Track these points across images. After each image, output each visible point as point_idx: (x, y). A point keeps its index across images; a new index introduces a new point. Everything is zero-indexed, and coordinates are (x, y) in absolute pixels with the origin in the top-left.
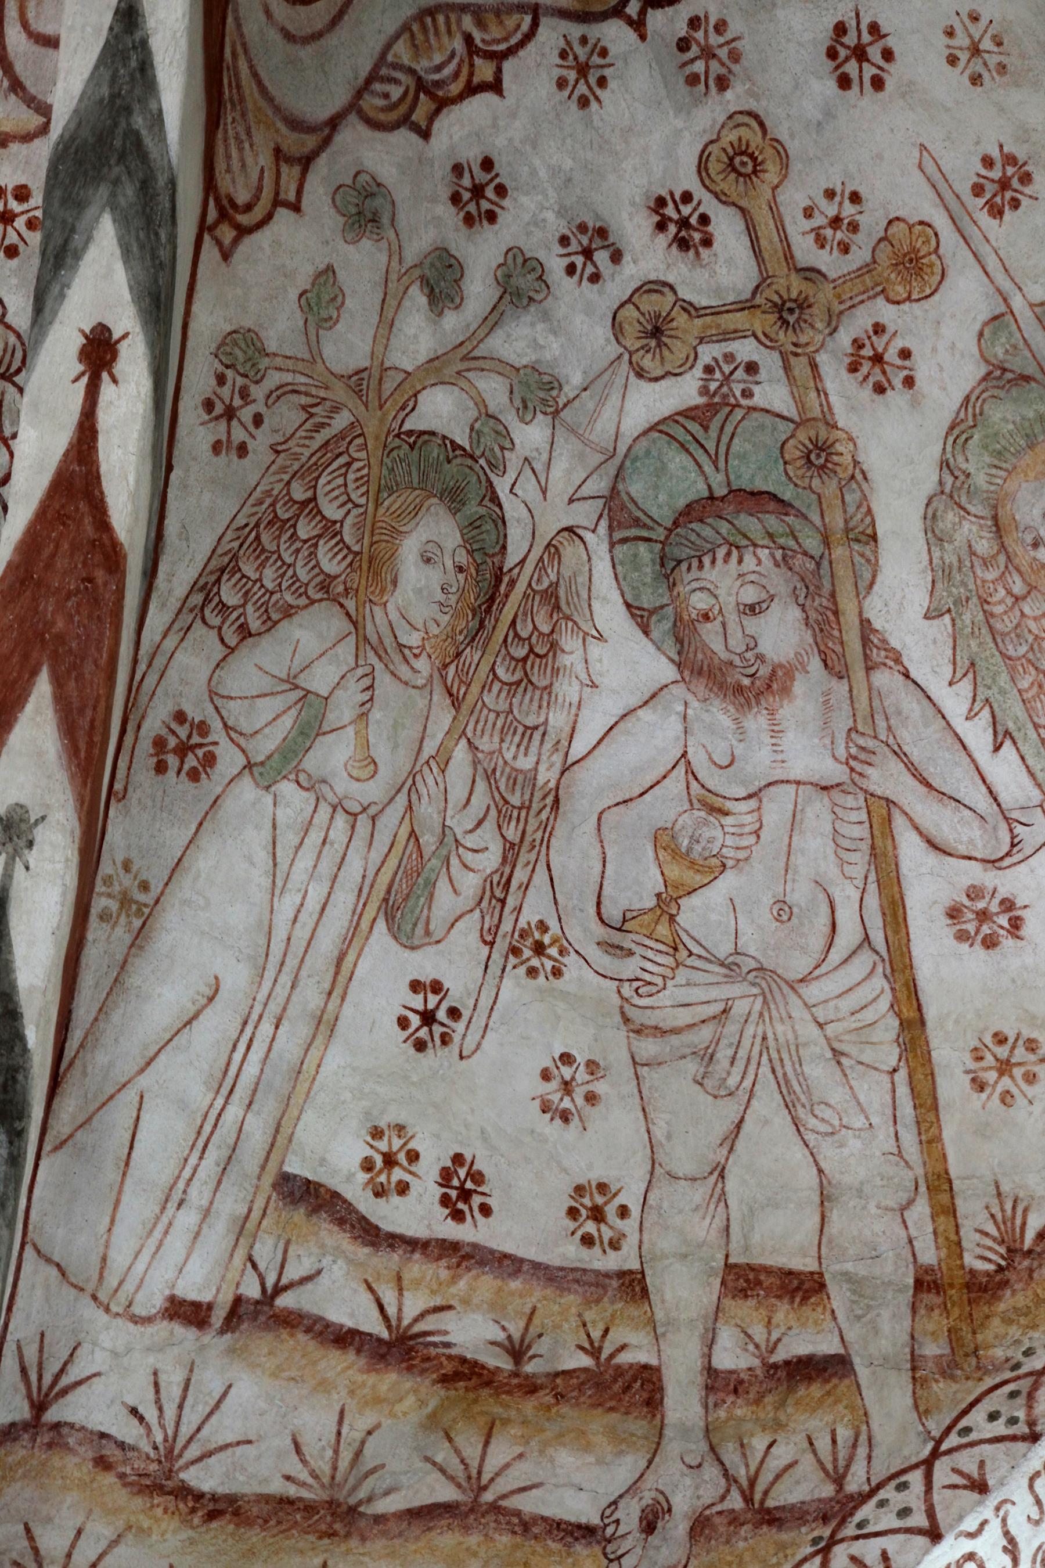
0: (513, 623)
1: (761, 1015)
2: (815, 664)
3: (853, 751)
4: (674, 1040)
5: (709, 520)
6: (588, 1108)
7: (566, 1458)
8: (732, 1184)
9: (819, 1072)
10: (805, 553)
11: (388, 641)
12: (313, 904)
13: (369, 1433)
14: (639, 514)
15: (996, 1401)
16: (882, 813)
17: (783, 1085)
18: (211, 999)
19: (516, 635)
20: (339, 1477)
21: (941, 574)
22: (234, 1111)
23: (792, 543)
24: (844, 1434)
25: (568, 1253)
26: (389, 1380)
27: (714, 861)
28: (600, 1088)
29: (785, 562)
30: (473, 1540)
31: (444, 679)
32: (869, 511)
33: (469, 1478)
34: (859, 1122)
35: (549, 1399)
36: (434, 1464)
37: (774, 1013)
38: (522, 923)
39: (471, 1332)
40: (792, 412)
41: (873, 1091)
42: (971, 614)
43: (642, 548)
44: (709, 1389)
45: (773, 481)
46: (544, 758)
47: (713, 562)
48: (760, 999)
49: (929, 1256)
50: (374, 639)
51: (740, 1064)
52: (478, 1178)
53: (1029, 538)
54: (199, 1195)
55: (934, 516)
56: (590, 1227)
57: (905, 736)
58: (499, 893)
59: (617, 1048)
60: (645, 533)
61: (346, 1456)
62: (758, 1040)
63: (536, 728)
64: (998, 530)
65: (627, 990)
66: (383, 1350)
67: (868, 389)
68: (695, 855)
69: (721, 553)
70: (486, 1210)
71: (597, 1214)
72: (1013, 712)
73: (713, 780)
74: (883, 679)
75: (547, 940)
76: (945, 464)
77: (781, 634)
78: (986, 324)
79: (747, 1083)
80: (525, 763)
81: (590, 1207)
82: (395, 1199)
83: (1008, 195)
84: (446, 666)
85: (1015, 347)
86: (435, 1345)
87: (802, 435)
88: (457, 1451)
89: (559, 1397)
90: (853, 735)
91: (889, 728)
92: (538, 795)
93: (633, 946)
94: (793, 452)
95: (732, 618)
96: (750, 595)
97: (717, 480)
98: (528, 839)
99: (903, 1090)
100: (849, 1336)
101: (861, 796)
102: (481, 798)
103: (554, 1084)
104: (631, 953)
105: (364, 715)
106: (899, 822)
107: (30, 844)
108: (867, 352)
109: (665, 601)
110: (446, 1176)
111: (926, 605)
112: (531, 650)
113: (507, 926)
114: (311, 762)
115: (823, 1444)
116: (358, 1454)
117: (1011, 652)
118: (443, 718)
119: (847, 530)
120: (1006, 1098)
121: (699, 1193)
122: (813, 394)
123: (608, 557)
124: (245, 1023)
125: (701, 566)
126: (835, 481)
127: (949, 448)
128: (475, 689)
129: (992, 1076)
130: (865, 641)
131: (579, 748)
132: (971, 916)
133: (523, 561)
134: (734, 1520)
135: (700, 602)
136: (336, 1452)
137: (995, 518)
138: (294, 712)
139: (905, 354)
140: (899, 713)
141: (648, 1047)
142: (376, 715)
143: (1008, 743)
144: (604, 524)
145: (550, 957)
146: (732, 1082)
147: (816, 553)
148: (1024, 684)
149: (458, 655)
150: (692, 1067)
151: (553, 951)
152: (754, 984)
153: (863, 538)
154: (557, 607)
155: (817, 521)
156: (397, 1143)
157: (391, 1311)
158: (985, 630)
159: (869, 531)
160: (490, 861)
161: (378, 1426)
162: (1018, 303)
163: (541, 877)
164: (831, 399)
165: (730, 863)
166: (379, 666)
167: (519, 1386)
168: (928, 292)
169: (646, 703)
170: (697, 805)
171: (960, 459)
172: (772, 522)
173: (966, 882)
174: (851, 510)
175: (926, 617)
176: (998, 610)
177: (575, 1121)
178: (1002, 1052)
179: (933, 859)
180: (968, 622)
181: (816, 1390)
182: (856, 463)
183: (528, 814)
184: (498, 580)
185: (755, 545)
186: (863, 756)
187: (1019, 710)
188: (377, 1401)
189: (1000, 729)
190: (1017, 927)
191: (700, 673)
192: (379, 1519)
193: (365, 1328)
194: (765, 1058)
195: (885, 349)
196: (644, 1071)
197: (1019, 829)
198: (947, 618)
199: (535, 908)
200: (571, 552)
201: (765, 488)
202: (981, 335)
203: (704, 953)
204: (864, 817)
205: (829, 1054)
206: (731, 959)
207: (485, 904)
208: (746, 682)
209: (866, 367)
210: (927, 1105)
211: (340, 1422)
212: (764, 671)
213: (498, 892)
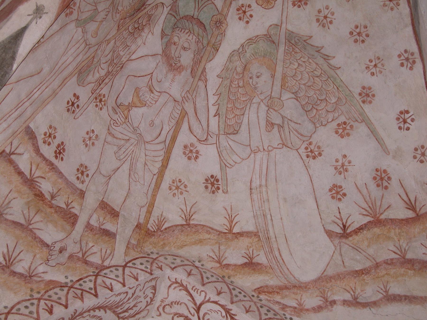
0: (139, 18)
1: (135, 145)
2: (189, 71)
3: (186, 96)
4: (115, 140)
5: (189, 22)
6: (91, 146)
7: (51, 227)
8: (111, 181)
9: (140, 165)
10: (202, 44)
11: (116, 6)
12: (68, 62)
13: (14, 199)
14: (177, 10)
15: (143, 260)
16: (184, 114)
17: (131, 164)
18: (39, 73)
19: (138, 21)
20: (3, 205)
21: (226, 69)
22: (27, 104)
23: (201, 39)
24: (108, 252)
25: (72, 179)
26: (25, 189)
27: (144, 102)
28: (96, 142)
29: (197, 43)
30: (23, 235)
31: (120, 22)
32: (220, 44)
33: (29, 220)
34: (142, 182)
35: (53, 211)
36: (23, 213)
37: (138, 146)
38: (101, 93)
39: (46, 187)
40: (220, 10)
41: (148, 177)
42: (227, 82)
43: (173, 18)
44: (86, 227)
45: (206, 22)
46: (126, 55)
47: (184, 32)
48: (137, 141)
49: (141, 221)
50: (115, 4)
51: (125, 154)
52: (64, 150)
53: (250, 75)
54: (10, 120)
55: (233, 55)
56: (80, 175)
57: (198, 101)
58: (100, 82)
59: (103, 134)
60: (176, 16)
61: (7, 201)
62: (132, 150)
63: (128, 46)
64: (245, 69)
65: (112, 122)
66: (26, 181)
67: (237, 17)
68: (141, 98)
69: (187, 31)
70: (62, 159)
71: (82, 173)
72: (223, 111)
73: (155, 83)
74: (201, 83)
75: (103, 100)
76: (242, 46)
77: (186, 59)
78: (274, 25)
79: (124, 159)
80: (122, 53)
81: (82, 170)
82: (47, 146)
83: (299, 3)
84: (122, 19)
85: (276, 34)
86: (38, 186)
87: (218, 17)
88: (29, 213)
89: (56, 212)
90: (188, 92)
91: (196, 96)
92: (120, 63)
93: (118, 112)
94: (214, 19)
95: (179, 47)
96: (186, 45)
97: (196, 13)
98: (113, 73)
99: (154, 180)
100: (119, 230)
101: (181, 108)
102: (109, 57)
103: (88, 136)
104: (117, 114)
105: (102, 21)
106: (186, 119)
107: (40, 17)
108: (243, 9)
109: (170, 34)
110: (59, 146)
111: (219, 73)
112: (138, 27)
113: (97, 91)
114: (87, 26)
115: (104, 251)
116: (10, 202)
117: (231, 97)
118: (114, 32)
119: (214, 45)
120: (174, 195)
121: (104, 180)
122: (226, 9)
123: (165, 16)
124: (41, 83)
125: (181, 31)
126: (218, 32)
127: (246, 43)
128: (123, 29)
129: (174, 188)
130: (202, 73)
131: (133, 57)
132: (188, 150)
133: (150, 5)
134: (79, 259)
135: (176, 39)
136: (5, 199)
137: (246, 66)
138: (92, 12)
139: (251, 16)
140: (200, 94)
141: (110, 139)
142: (104, 23)
143: (218, 116)
144: (170, 7)
145: (102, 104)
146: (122, 157)
147: (204, 46)
148: (229, 106)
149: (125, 18)
150: (115, 148)
151: (103, 103)
152: (137, 137)
153: (215, 49)
154: (149, 20)
155: (209, 39)
156: (53, 132)
157: (33, 172)
158: (228, 88)
159: (217, 48)
160: (103, 73)
161: (17, 198)
162: (284, 26)
163: (110, 84)
164: (229, 13)
165: (147, 105)
166: (111, 11)
167: (49, 205)
168: (266, 8)
169: (152, 56)
170: (148, 87)
171: (247, 47)
172: (201, 31)
173: (192, 141)
174: (217, 41)
175: (217, 76)
176: (234, 86)
177: (88, 148)
178: (179, 184)
179: (188, 132)
180: (225, 84)
181: (107, 239)
182: (225, 31)
183: (116, 66)
184: (143, 6)
185: (194, 34)
186: (187, 98)
187: (224, 111)
188: (19, 192)
189: (218, 112)
190: (196, 159)
191: (166, 56)
192: (6, 220)
193: (26, 173)
194: (131, 156)
195: (248, 11)
196: (106, 143)
197: (209, 137)
198: (221, 80)
199: (105, 91)
200: (160, 9)
201: (204, 23)
202: (271, 26)
203: (131, 123)
204: (179, 113)
205: (144, 163)
206: (136, 128)
207: (97, 82)
208: (174, 65)
209: (241, 12)
210: (158, 186)
211: (9, 193)
212: (178, 65)
213: (101, 82)
